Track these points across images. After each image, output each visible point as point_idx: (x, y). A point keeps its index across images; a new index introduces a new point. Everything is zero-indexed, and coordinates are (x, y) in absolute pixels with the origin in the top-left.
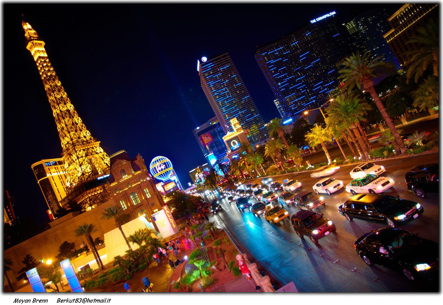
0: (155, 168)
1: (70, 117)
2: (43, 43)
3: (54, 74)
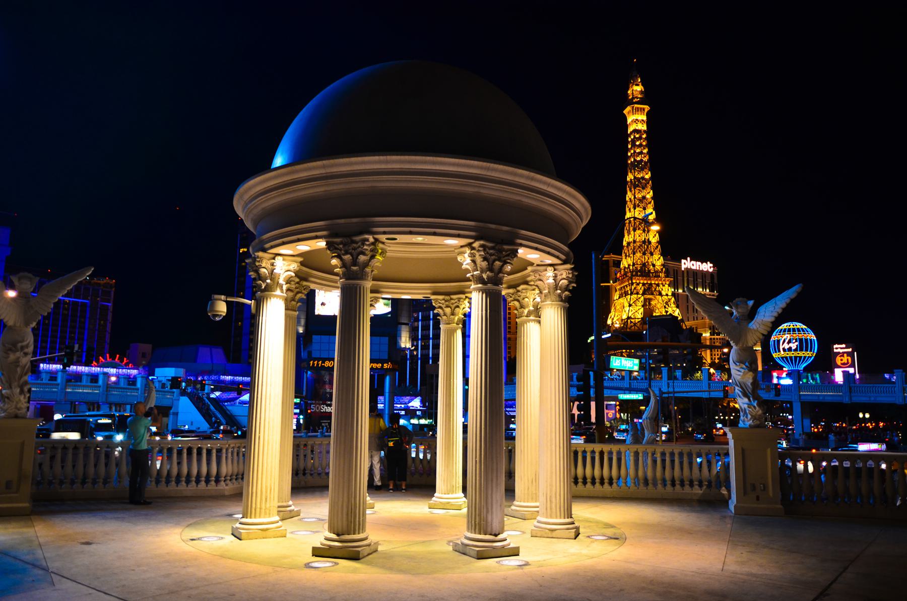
0: (779, 341)
1: (644, 231)
2: (647, 108)
3: (646, 159)
